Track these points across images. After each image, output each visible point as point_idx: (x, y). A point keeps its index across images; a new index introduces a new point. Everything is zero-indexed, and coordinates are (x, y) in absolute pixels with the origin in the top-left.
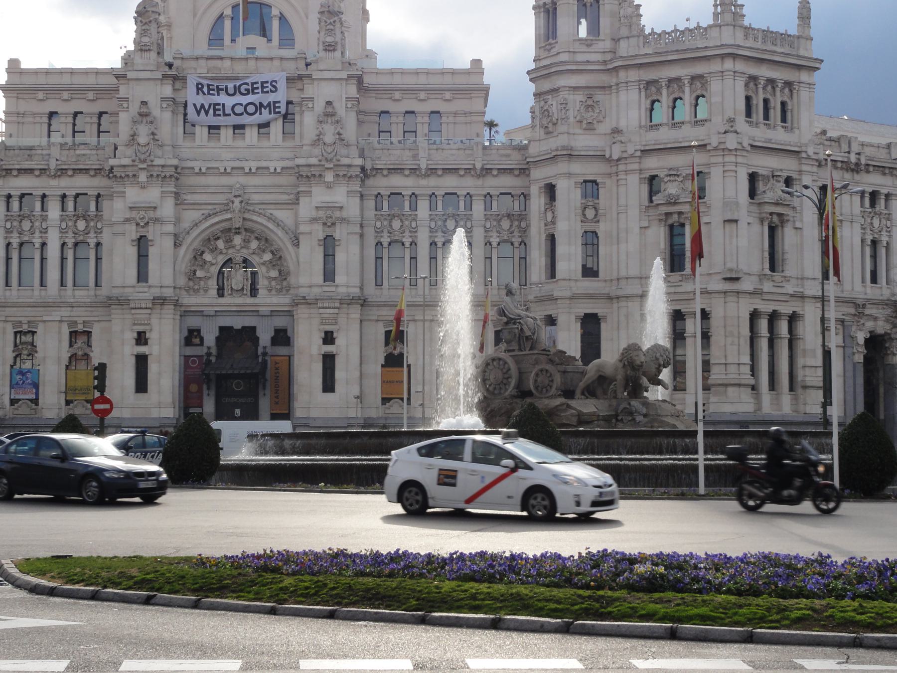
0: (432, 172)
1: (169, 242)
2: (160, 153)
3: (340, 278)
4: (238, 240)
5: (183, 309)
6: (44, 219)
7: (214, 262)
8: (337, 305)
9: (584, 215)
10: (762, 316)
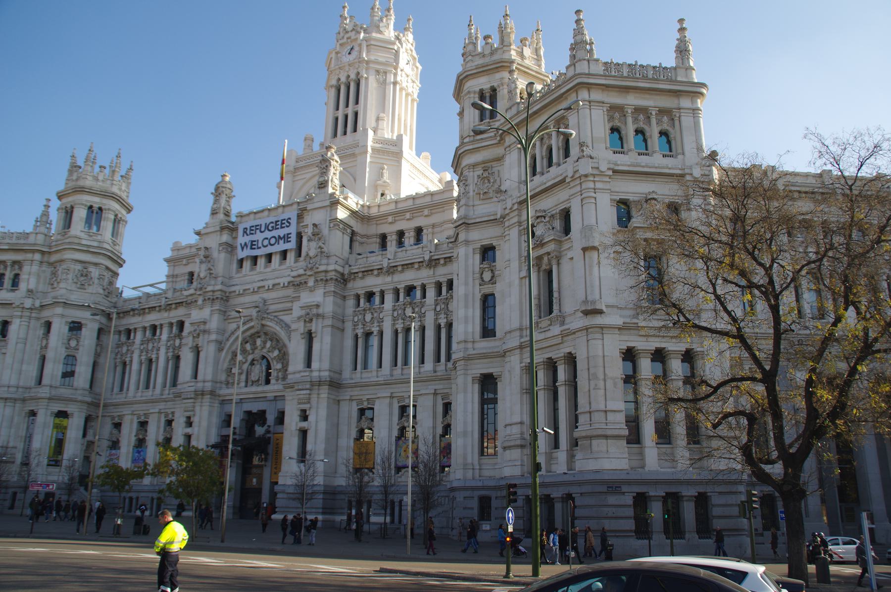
0: (392, 270)
1: (212, 348)
2: (213, 282)
3: (315, 365)
4: (259, 342)
5: (221, 398)
6: (160, 339)
7: (244, 360)
8: (308, 386)
9: (482, 278)
10: (641, 355)
